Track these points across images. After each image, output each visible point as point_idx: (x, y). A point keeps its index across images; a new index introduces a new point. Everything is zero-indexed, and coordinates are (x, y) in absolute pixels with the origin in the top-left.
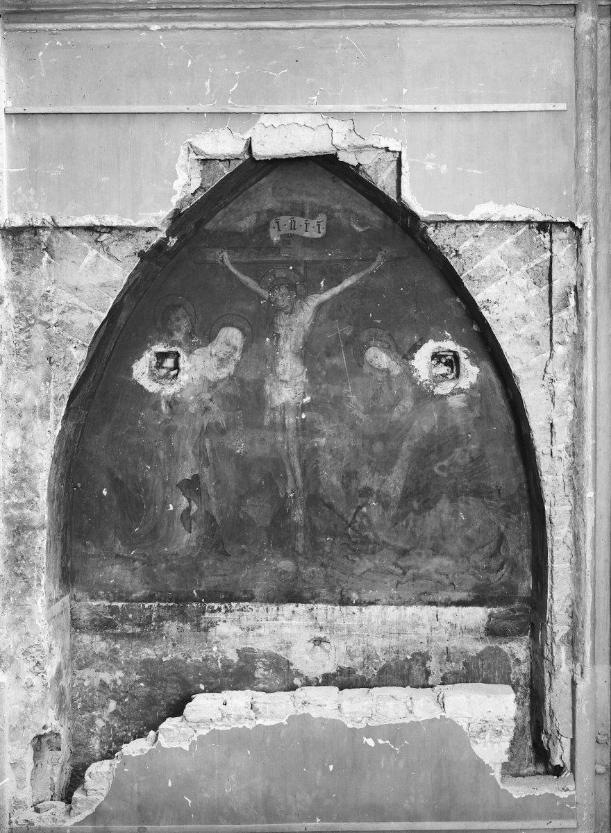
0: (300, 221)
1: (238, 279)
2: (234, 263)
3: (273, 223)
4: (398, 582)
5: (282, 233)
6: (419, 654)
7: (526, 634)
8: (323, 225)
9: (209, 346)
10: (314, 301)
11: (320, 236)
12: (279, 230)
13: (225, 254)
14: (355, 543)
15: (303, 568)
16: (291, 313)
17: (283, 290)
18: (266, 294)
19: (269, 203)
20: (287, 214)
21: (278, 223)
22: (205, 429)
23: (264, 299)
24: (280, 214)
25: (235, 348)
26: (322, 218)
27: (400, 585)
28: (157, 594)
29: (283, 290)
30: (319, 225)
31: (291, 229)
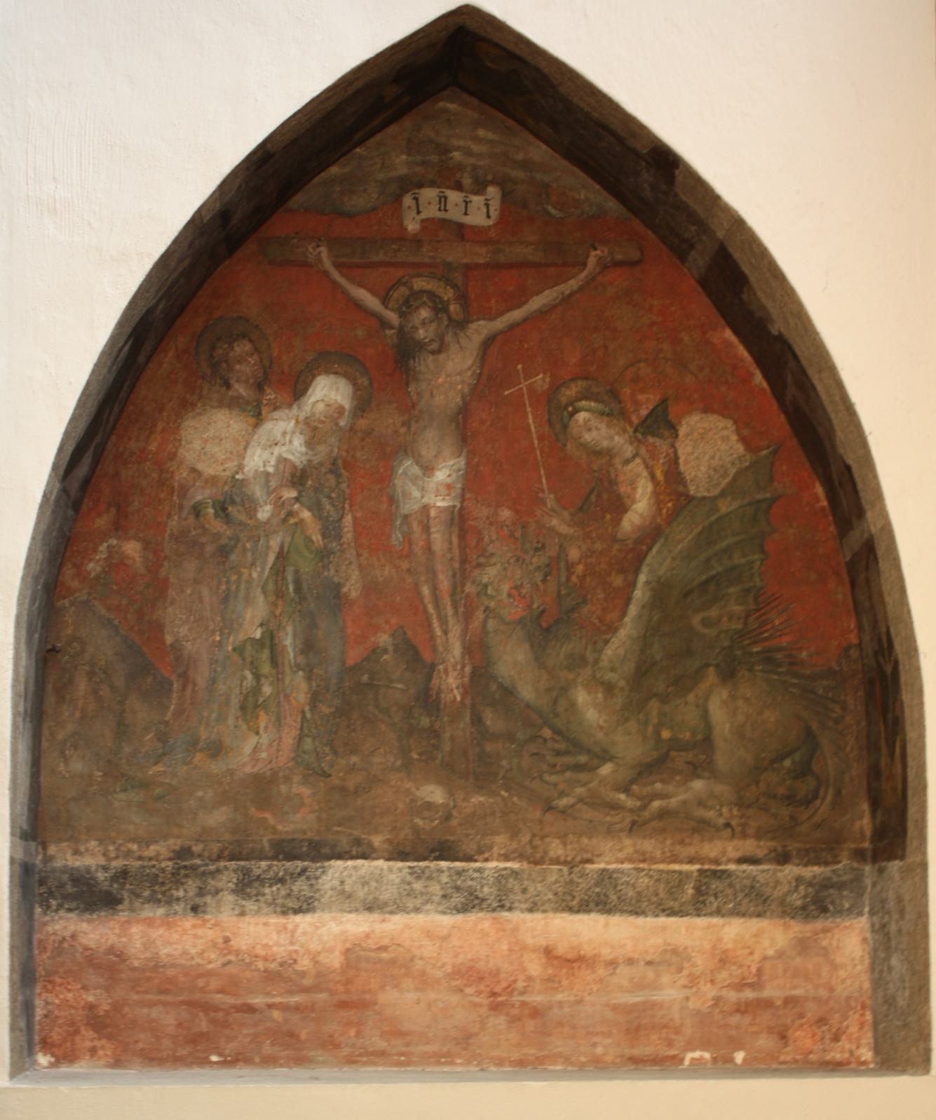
0: (454, 197)
1: (345, 293)
2: (337, 266)
3: (408, 200)
4: (634, 823)
5: (423, 216)
6: (675, 952)
7: (860, 914)
8: (495, 206)
9: (295, 406)
10: (481, 329)
11: (490, 222)
12: (419, 212)
13: (324, 251)
14: (558, 753)
15: (462, 797)
16: (439, 351)
17: (425, 313)
18: (393, 317)
19: (401, 164)
20: (433, 184)
21: (416, 199)
22: (285, 550)
23: (392, 328)
24: (420, 186)
25: (341, 411)
26: (492, 191)
27: (635, 828)
28: (196, 845)
29: (425, 313)
30: (487, 205)
31: (440, 210)
